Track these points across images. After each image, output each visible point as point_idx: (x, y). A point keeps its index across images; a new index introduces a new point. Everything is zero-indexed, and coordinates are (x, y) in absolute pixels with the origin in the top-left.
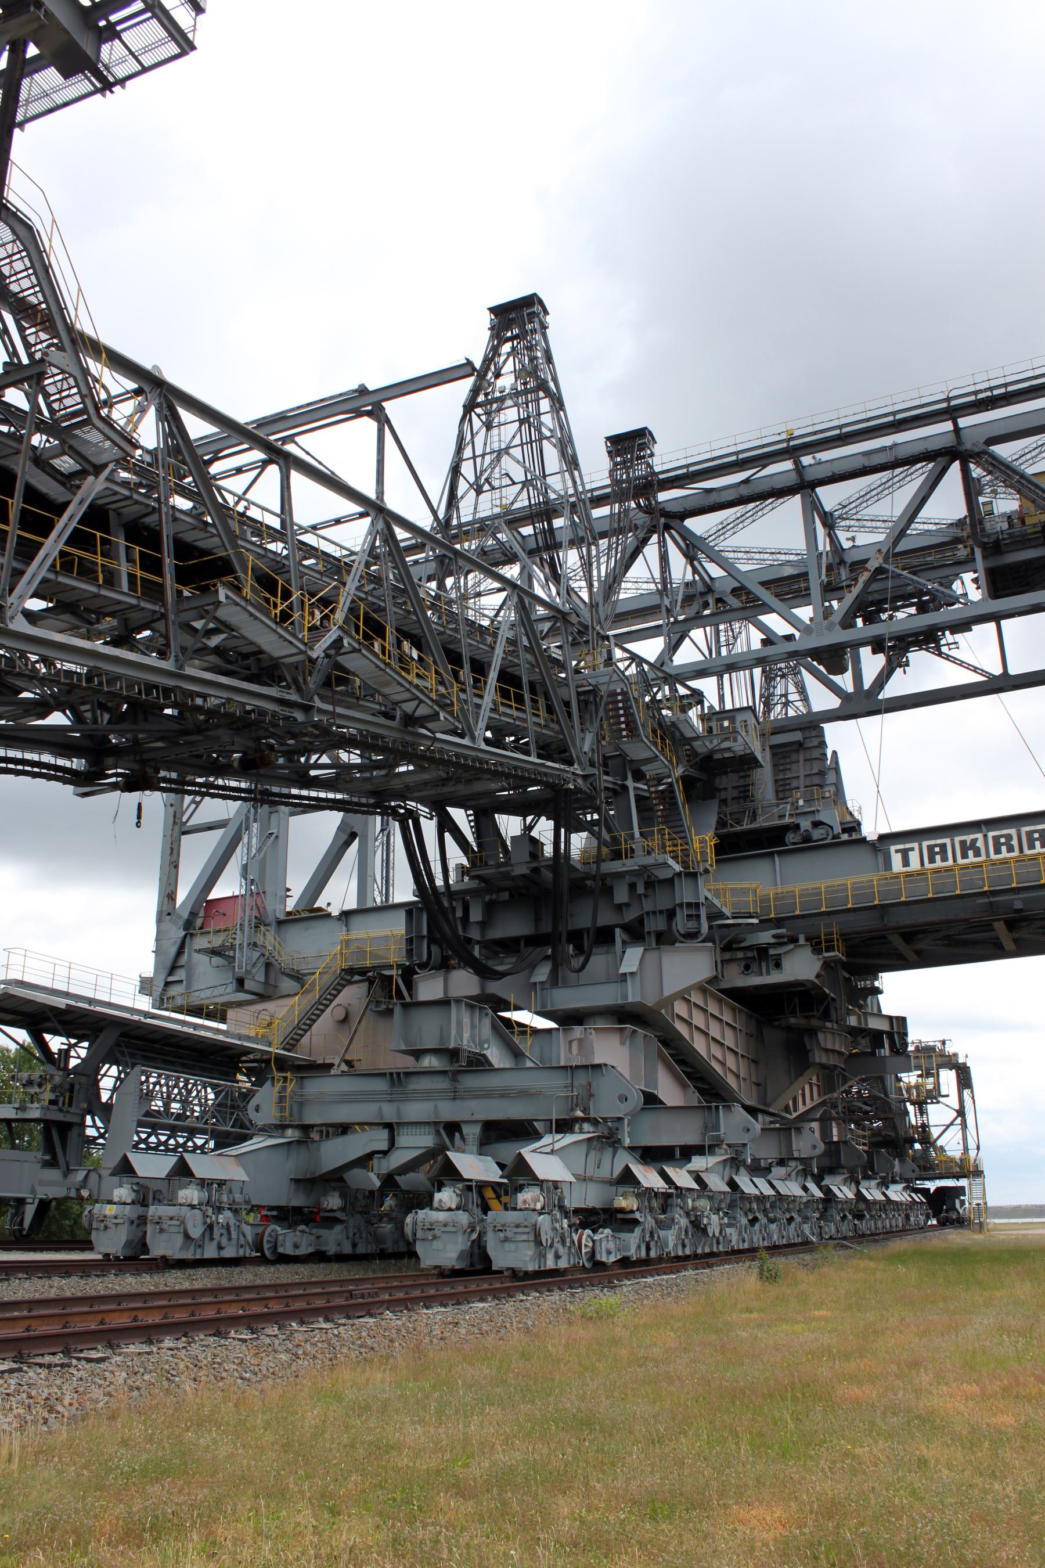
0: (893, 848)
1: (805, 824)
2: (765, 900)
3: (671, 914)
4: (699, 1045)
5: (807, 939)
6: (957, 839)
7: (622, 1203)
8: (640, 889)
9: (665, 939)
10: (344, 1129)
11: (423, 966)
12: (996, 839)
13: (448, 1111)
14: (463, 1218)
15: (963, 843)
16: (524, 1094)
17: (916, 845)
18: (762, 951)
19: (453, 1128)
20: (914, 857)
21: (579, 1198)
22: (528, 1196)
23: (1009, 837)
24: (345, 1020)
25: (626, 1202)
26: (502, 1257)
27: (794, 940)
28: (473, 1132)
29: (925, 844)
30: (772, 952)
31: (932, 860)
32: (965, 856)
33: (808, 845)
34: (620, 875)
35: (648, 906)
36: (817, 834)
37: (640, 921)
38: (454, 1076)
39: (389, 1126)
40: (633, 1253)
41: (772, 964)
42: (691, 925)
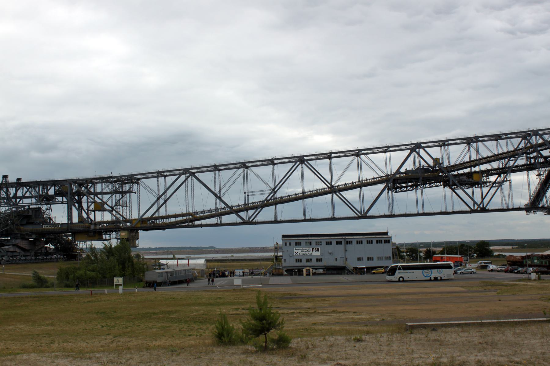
1: (35, 222)
3: (17, 237)
4: (21, 246)
9: (17, 239)
20: (45, 227)
21: (6, 260)
22: (3, 260)
25: (10, 260)
27: (33, 234)
33: (35, 224)
36: (37, 223)
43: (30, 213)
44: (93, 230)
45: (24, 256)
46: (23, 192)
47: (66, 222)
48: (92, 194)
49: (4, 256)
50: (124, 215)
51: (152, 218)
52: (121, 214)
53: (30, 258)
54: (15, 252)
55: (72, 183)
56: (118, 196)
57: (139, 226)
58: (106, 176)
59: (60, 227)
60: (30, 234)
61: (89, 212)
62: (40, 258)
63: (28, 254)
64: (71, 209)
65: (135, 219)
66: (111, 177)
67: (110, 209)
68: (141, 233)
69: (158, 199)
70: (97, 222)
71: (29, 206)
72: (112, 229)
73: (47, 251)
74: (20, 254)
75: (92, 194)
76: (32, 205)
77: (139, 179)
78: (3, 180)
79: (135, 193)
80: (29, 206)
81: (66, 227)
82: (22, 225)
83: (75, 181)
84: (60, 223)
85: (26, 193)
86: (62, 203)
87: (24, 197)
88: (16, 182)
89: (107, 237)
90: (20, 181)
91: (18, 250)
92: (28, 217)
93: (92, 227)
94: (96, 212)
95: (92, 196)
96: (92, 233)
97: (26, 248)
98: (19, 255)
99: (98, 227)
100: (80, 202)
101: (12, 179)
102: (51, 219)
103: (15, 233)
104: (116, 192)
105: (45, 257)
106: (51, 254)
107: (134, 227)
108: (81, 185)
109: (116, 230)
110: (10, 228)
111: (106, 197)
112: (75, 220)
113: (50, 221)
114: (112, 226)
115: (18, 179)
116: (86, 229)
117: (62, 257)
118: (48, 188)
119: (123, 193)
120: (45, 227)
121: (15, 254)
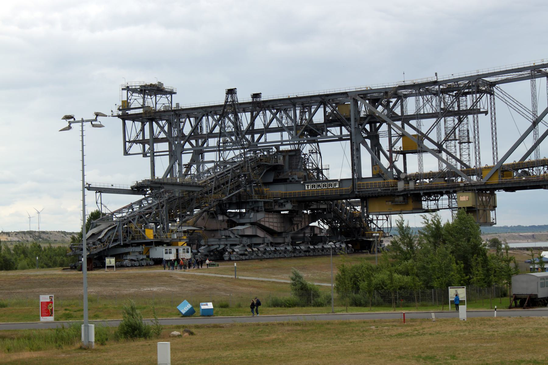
0: (306, 185)
1: (290, 179)
2: (282, 194)
3: (258, 207)
4: (267, 225)
5: (290, 201)
6: (317, 184)
7: (246, 253)
8: (253, 203)
9: (258, 211)
10: (213, 245)
11: (219, 214)
12: (324, 184)
13: (226, 243)
14: (228, 255)
15: (318, 185)
16: (235, 241)
17: (310, 185)
18: (282, 204)
19: (227, 245)
20: (309, 187)
21: (240, 253)
22: (234, 253)
23: (326, 184)
24: (204, 219)
25: (246, 253)
26: (232, 258)
27: (287, 202)
28: (229, 245)
29: (311, 184)
30: (283, 204)
31: (312, 188)
32: (318, 187)
33: (291, 182)
34: (250, 201)
35: (255, 205)
36: (293, 180)
37: (253, 208)
38: (226, 239)
39: (219, 245)
40: (247, 258)
41: (283, 206)
42: (261, 209)
43: (281, 161)
44: (402, 191)
45: (272, 244)
46: (265, 121)
47: (351, 177)
48: (396, 118)
49: (236, 245)
50: (465, 159)
51: (521, 165)
52: (458, 157)
53: (283, 248)
54: (256, 236)
55: (358, 98)
56: (451, 121)
57: (496, 180)
58: (425, 81)
59: (337, 186)
60: (282, 201)
61: (394, 155)
62: (303, 247)
63: (280, 240)
64: (358, 150)
65: (487, 168)
66: (435, 83)
67: (436, 148)
68: (501, 196)
69: (535, 124)
70: (410, 176)
71: (277, 147)
72: (441, 188)
73: (315, 235)
74: (264, 240)
75: (396, 118)
76: (282, 145)
77: (493, 84)
78: (227, 99)
79: (486, 113)
80: (277, 147)
81: (348, 187)
82: (266, 184)
83: (364, 95)
84: (339, 178)
85: (271, 121)
86: (340, 139)
87: (267, 130)
88: (251, 101)
89: (432, 205)
90: (258, 99)
91: (260, 233)
92: (276, 169)
93: (401, 185)
94: (408, 155)
95: (399, 123)
96: (401, 199)
97: (276, 229)
98: (263, 244)
99: (411, 185)
100: (374, 137)
101: (243, 97)
102: (319, 171)
103: (254, 200)
104: (446, 113)
105: (312, 247)
106: (323, 240)
107: (485, 184)
108: (375, 102)
109: (448, 190)
110: (245, 190)
111: (426, 125)
112: (367, 172)
113: (318, 175)
114: (440, 183)
115: (254, 94)
116: (389, 189)
117: (344, 246)
118: (313, 110)
119: (461, 114)
120: (309, 187)
121: (256, 241)
